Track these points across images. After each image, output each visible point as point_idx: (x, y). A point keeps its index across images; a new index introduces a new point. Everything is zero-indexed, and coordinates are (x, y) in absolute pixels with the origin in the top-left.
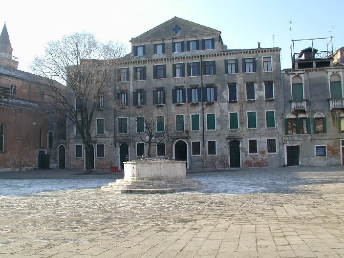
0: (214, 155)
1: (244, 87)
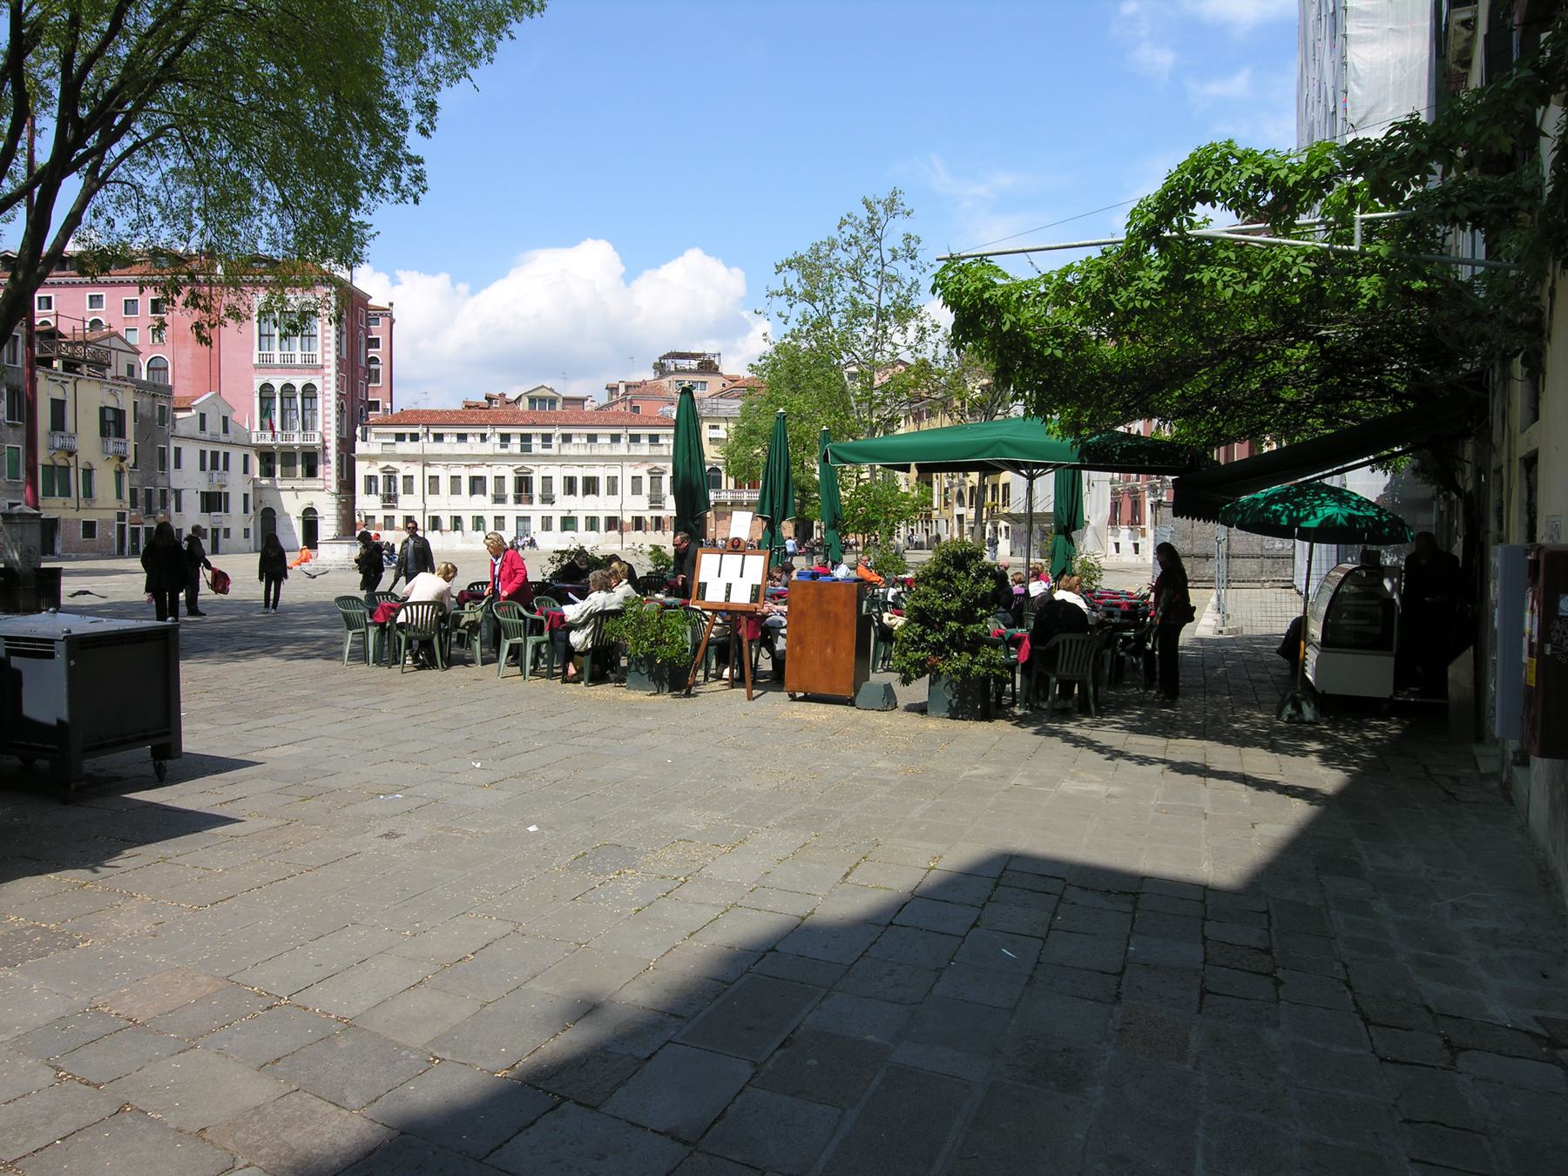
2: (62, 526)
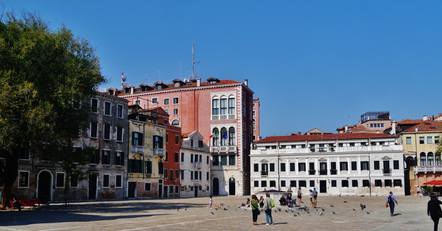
0: (76, 187)
1: (103, 127)
2: (137, 185)
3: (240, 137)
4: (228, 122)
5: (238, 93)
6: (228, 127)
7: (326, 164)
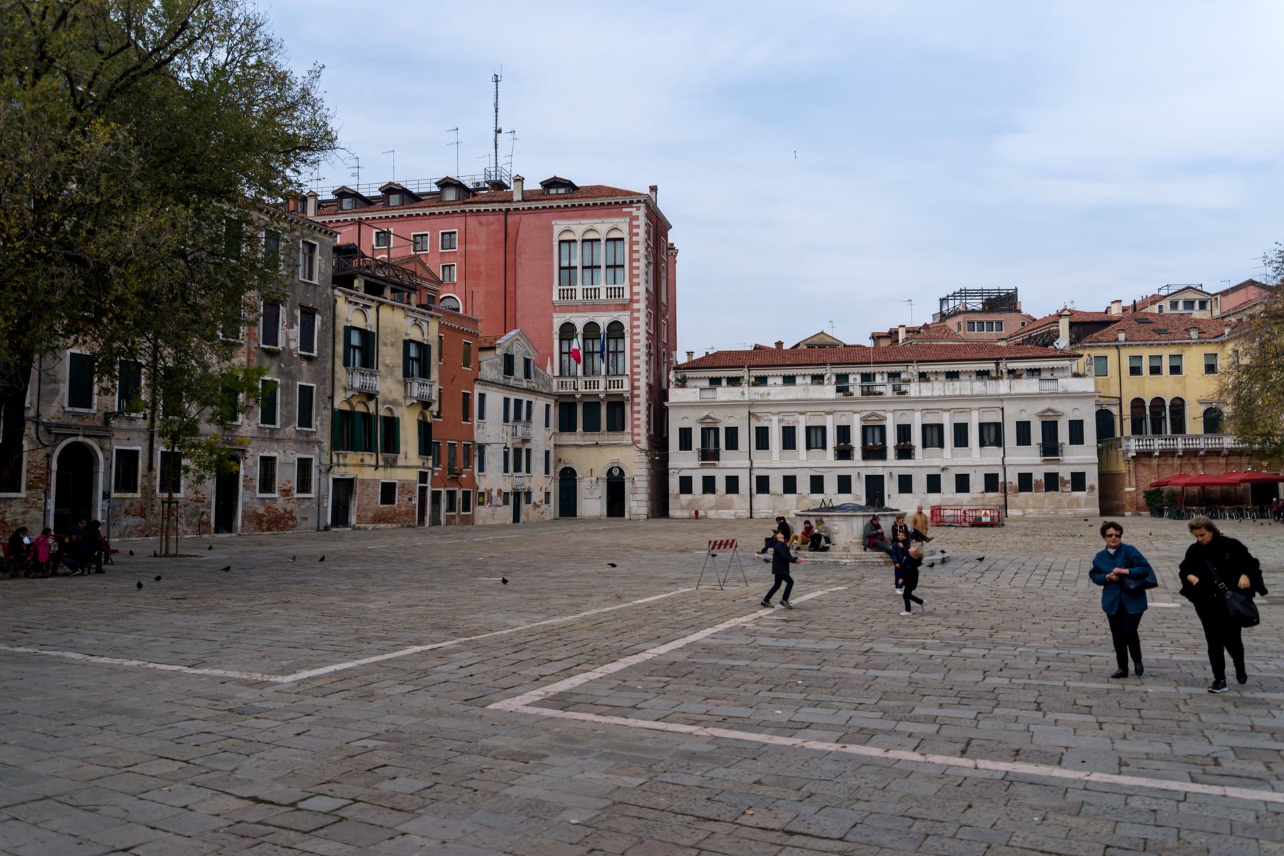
3: (639, 350)
4: (605, 308)
5: (635, 223)
6: (603, 320)
7: (882, 429)
